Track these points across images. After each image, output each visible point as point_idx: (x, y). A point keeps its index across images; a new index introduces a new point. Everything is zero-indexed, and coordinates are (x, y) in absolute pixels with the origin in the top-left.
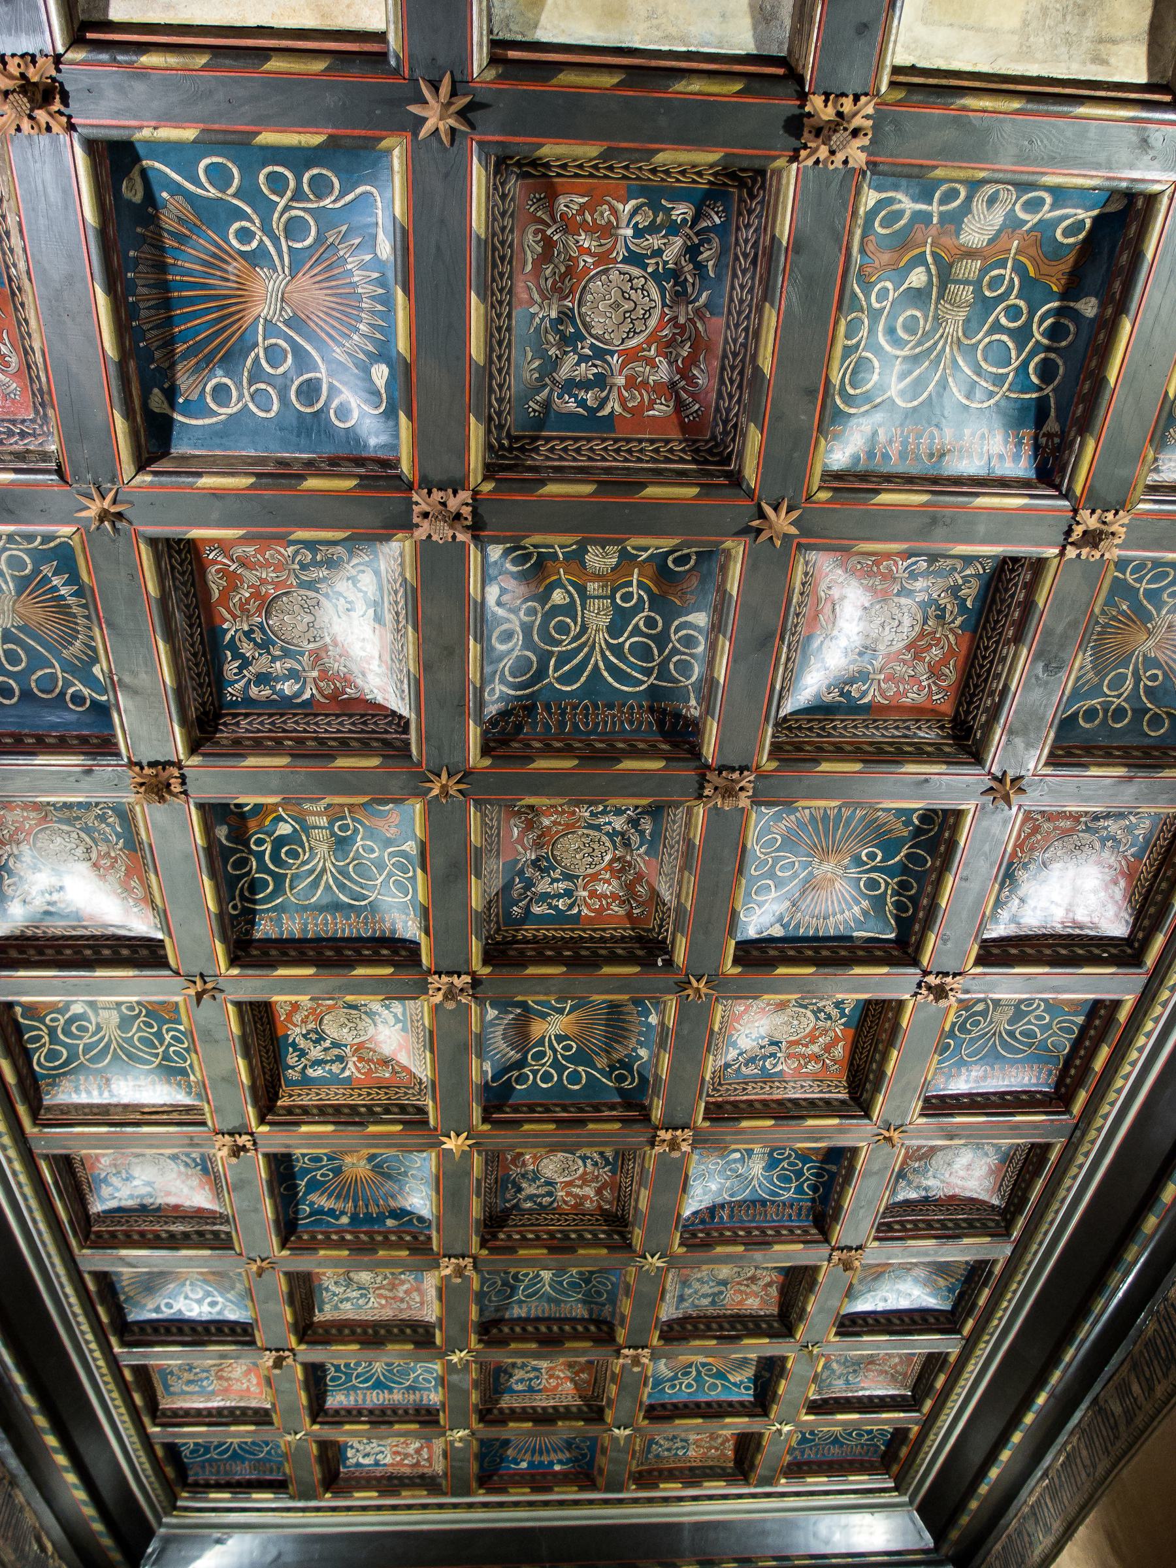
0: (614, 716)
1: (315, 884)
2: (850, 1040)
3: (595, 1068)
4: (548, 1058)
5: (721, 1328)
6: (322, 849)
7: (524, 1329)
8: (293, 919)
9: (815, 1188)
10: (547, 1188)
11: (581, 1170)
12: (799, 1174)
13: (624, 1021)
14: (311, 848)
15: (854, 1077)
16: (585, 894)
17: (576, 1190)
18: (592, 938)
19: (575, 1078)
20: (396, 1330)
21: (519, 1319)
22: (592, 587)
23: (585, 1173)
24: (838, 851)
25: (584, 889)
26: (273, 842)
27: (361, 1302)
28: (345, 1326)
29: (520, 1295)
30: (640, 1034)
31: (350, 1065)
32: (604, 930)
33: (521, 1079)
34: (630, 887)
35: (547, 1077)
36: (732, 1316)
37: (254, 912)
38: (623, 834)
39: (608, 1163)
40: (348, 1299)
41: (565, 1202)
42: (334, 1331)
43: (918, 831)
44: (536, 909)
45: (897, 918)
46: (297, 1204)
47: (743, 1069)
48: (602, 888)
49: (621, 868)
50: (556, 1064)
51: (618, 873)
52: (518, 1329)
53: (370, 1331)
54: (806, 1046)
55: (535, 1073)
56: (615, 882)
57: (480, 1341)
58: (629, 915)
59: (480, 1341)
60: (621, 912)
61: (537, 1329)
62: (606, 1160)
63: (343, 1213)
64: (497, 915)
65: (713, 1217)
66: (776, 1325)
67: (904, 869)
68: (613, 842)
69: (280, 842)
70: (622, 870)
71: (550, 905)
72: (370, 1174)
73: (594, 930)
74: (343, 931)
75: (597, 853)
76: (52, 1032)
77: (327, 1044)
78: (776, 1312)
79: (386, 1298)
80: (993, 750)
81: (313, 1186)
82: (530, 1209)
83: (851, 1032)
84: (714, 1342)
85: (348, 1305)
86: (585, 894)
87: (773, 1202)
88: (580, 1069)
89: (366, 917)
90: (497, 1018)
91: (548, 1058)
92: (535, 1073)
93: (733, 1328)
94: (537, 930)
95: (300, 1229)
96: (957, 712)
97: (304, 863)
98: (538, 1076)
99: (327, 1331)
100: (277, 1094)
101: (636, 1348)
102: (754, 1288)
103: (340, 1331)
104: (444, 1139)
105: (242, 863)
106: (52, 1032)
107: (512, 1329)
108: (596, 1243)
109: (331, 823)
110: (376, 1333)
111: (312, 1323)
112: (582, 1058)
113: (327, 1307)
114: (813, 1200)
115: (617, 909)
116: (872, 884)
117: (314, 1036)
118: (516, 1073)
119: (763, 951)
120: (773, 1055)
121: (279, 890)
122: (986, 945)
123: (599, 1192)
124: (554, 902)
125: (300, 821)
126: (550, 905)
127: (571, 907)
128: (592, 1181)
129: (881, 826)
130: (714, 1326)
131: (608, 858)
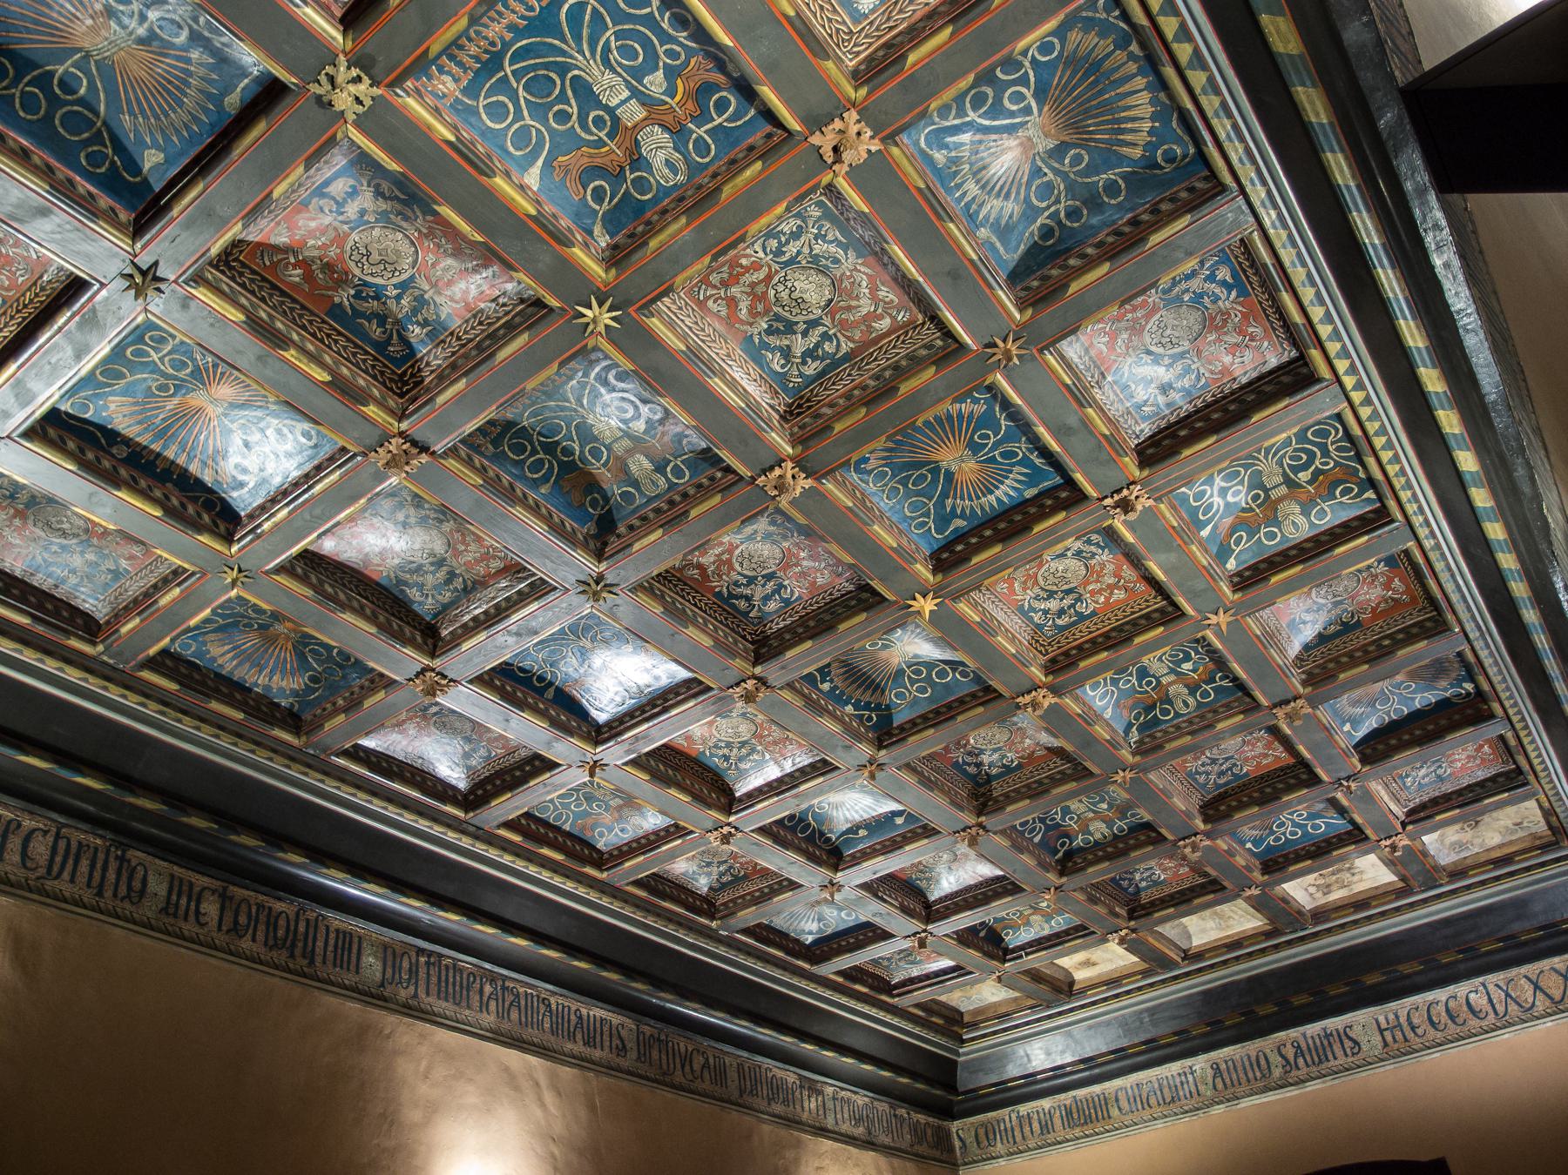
13: (859, 686)
22: (1091, 815)
23: (731, 568)
27: (774, 243)
30: (842, 693)
40: (795, 235)
62: (737, 597)
69: (1187, 658)
72: (934, 457)
76: (1325, 453)
77: (1069, 554)
79: (747, 269)
106: (1325, 453)
109: (1159, 682)
113: (815, 213)
125: (1178, 674)
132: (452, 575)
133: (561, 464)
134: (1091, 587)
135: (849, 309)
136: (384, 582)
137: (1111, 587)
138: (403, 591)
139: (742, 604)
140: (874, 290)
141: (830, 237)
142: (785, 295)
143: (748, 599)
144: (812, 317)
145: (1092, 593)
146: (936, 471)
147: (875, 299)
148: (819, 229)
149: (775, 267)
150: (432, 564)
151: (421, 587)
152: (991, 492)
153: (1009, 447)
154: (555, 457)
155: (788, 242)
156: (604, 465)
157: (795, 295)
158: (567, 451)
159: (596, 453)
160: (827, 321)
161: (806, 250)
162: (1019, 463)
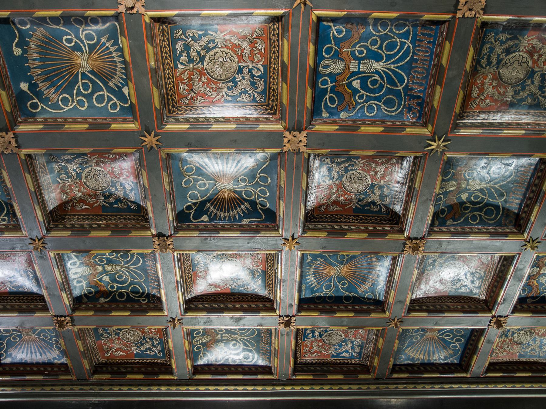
6: (116, 267)
10: (376, 189)
11: (362, 172)
24: (71, 59)
46: (364, 298)
47: (259, 90)
54: (243, 51)
55: (259, 197)
64: (135, 216)
65: (419, 97)
68: (87, 167)
69: (113, 280)
75: (97, 173)
87: (414, 53)
90: (209, 216)
97: (125, 274)
103: (493, 292)
105: (121, 295)
110: (500, 277)
118: (259, 206)
120: (250, 71)
132: (489, 63)
150: (502, 59)
151: (502, 42)
153: (333, 289)
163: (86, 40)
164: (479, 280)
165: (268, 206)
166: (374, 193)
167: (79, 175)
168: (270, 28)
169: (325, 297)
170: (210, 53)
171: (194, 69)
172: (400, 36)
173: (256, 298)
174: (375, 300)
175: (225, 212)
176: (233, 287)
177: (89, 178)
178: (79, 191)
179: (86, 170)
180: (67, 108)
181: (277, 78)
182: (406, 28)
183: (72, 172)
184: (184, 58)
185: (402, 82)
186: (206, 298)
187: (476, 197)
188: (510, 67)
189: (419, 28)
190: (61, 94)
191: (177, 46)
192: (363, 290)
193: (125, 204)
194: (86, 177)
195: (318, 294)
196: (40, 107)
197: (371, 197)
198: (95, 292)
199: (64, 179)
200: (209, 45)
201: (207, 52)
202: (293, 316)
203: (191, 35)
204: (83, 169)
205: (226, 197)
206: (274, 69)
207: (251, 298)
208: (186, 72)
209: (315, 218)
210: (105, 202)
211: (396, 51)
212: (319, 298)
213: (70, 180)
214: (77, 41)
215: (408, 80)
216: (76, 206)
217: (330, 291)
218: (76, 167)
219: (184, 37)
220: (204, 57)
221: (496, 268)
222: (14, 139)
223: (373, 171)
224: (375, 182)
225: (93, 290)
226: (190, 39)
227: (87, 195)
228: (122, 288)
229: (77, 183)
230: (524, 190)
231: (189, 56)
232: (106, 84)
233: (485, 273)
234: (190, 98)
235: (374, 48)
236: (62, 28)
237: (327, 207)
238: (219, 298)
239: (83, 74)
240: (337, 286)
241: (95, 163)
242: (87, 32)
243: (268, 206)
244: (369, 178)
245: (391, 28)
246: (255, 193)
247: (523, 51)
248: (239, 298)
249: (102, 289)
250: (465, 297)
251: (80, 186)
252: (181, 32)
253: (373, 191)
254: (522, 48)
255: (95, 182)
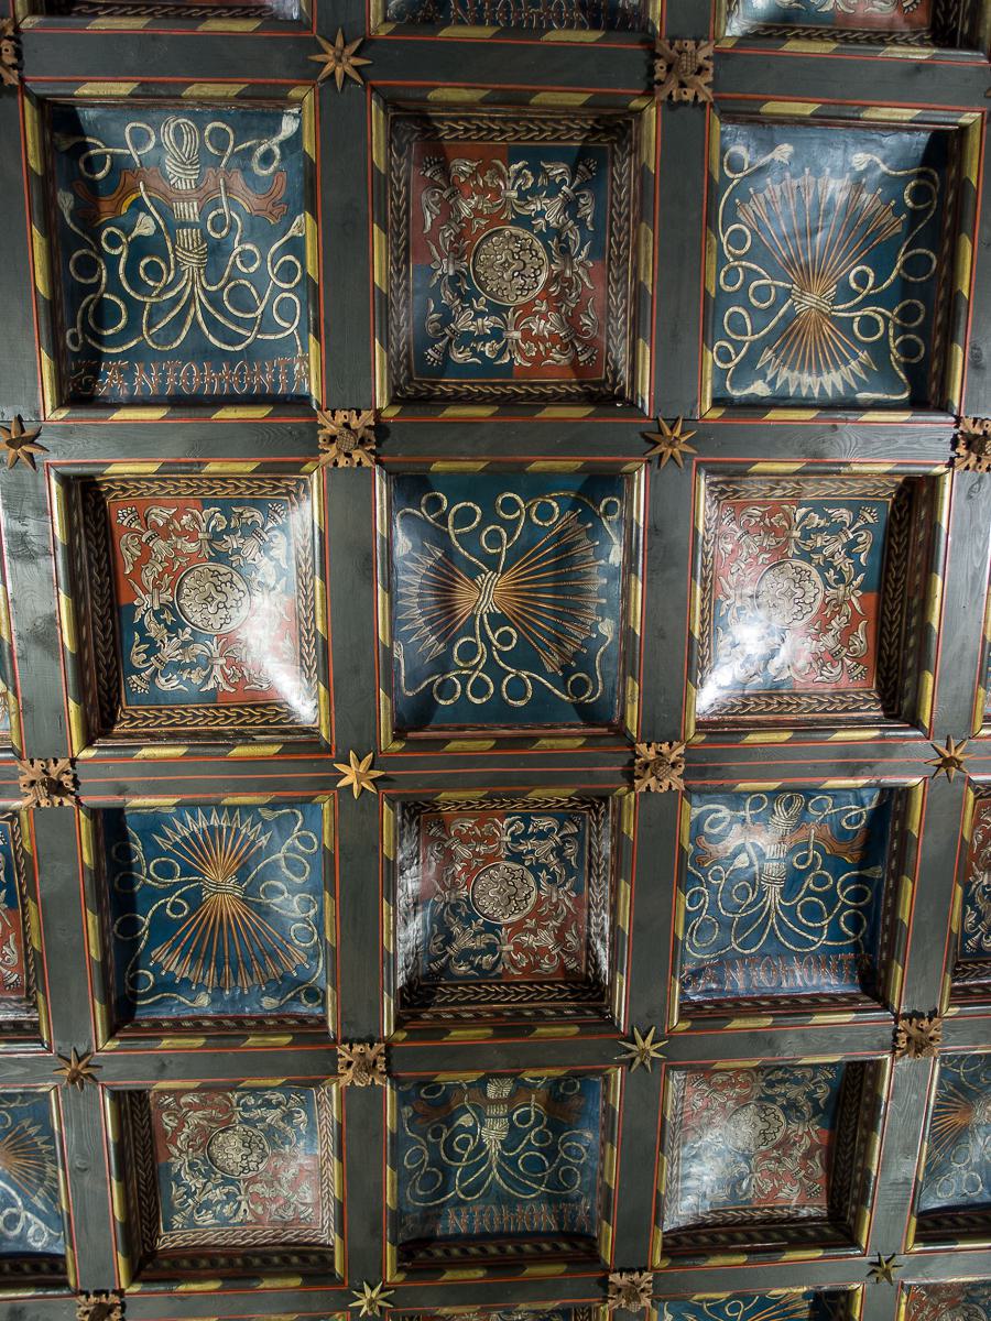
0: (540, 15)
1: (179, 321)
2: (872, 615)
3: (542, 672)
4: (480, 659)
5: (751, 1239)
6: (191, 264)
7: (464, 1251)
8: (148, 371)
9: (855, 923)
11: (532, 900)
12: (830, 898)
14: (177, 263)
15: (886, 679)
16: (517, 335)
17: (528, 939)
18: (529, 394)
19: (517, 688)
20: (276, 1260)
21: (458, 1236)
23: (539, 903)
25: (516, 329)
26: (131, 245)
27: (227, 1210)
28: (202, 1256)
29: (456, 1192)
31: (217, 671)
32: (544, 385)
33: (446, 689)
34: (571, 322)
35: (479, 689)
36: (763, 1222)
37: (99, 356)
38: (558, 232)
39: (570, 872)
40: (207, 1205)
41: (514, 963)
42: (185, 1263)
43: (915, 216)
44: (459, 356)
45: (907, 368)
46: (136, 967)
48: (539, 326)
49: (561, 292)
50: (490, 666)
51: (556, 302)
52: (455, 1252)
53: (239, 1261)
55: (464, 679)
56: (553, 317)
57: (400, 1269)
58: (574, 364)
59: (400, 1269)
60: (564, 360)
61: (483, 1250)
63: (201, 987)
66: (828, 1231)
67: (904, 288)
68: (547, 248)
69: (140, 247)
70: (561, 297)
71: (473, 350)
72: (240, 909)
73: (532, 385)
74: (212, 386)
75: (529, 271)
78: (825, 1213)
80: (935, 638)
81: (164, 929)
82: (466, 976)
83: (873, 597)
84: (743, 1259)
85: (207, 1219)
86: (517, 335)
88: (524, 674)
89: (241, 369)
91: (480, 659)
92: (464, 679)
93: (767, 1238)
94: (460, 384)
95: (139, 1015)
96: (935, 18)
97: (168, 287)
98: (467, 682)
99: (175, 1264)
100: (113, 713)
101: (631, 1271)
102: (789, 1164)
104: (341, 767)
105: (87, 266)
107: (447, 1252)
108: (561, 1018)
109: (203, 213)
110: (247, 1264)
111: (155, 1252)
112: (525, 657)
114: (856, 947)
115: (558, 357)
116: (869, 325)
117: (170, 619)
118: (438, 679)
119: (694, 1238)
121: (133, 329)
122: (924, 1216)
123: (560, 939)
124: (479, 347)
126: (473, 350)
127: (501, 353)
128: (548, 917)
129: (868, 222)
130: (740, 1236)
131: (543, 278)
132: (771, 1085)
133: (557, 1133)
134: (192, 547)
135: (211, 1120)
136: (828, 1122)
137: (163, 533)
138: (826, 1103)
139: (571, 851)
140: (178, 1129)
141: (183, 1190)
142: (254, 1157)
143: (559, 851)
144: (247, 1128)
145: (193, 538)
146: (251, 891)
147: (182, 1122)
148: (186, 1201)
149: (242, 1186)
152: (211, 828)
153: (159, 882)
154: (555, 1143)
155: (218, 1202)
156: (528, 1105)
157: (245, 1151)
158: (541, 1137)
159: (524, 1118)
160: (237, 1118)
161: (210, 1185)
162: (160, 852)
163: (862, 316)
164: (215, 1217)
165: (442, 702)
166: (474, 936)
167: (524, 222)
168: (868, 693)
169: (130, 867)
170: (815, 572)
171: (789, 538)
172: (834, 924)
173: (108, 679)
174: (135, 997)
175: (419, 595)
176: (140, 611)
177: (515, 247)
178: (474, 210)
179: (538, 244)
180: (724, 240)
181: (771, 712)
182: (851, 933)
183: (536, 206)
184: (816, 520)
185: (743, 945)
186: (97, 535)
187: (464, 1144)
188: (757, 1118)
189: (851, 955)
190: (750, 230)
191: (843, 510)
192: (168, 961)
193: (437, 331)
194: (517, 238)
195: (137, 847)
196: (731, 176)
197: (464, 929)
198: (94, 183)
199: (520, 181)
200: (832, 572)
201: (818, 566)
202: (77, 797)
203: (860, 540)
204: (540, 235)
205: (458, 596)
206: (789, 704)
207: (108, 667)
208: (785, 523)
209: (412, 817)
210: (443, 275)
211: (804, 921)
212: (126, 853)
213: (514, 194)
214: (860, 297)
215: (751, 954)
216: (433, 195)
217: (149, 876)
218: (551, 220)
219: (858, 525)
220: (810, 561)
221: (265, 1245)
222: (692, 100)
223: (538, 925)
224: (503, 933)
225: (100, 175)
226: (851, 536)
227: (462, 228)
228: (112, 270)
229: (502, 211)
230: (496, 1228)
231: (819, 530)
232: (766, 342)
233: (241, 1223)
234: (732, 529)
235: (809, 882)
236: (895, 273)
237: (440, 838)
238: (100, 573)
239: (788, 293)
240: (169, 892)
241: (563, 272)
242: (881, 324)
243: (442, 702)
244: (515, 918)
245: (850, 907)
246: (474, 668)
247: (788, 1129)
248: (104, 630)
249: (106, 206)
250: (156, 1204)
251: (490, 216)
252: (871, 520)
253: (481, 933)
254: (793, 1126)
255: (501, 259)
